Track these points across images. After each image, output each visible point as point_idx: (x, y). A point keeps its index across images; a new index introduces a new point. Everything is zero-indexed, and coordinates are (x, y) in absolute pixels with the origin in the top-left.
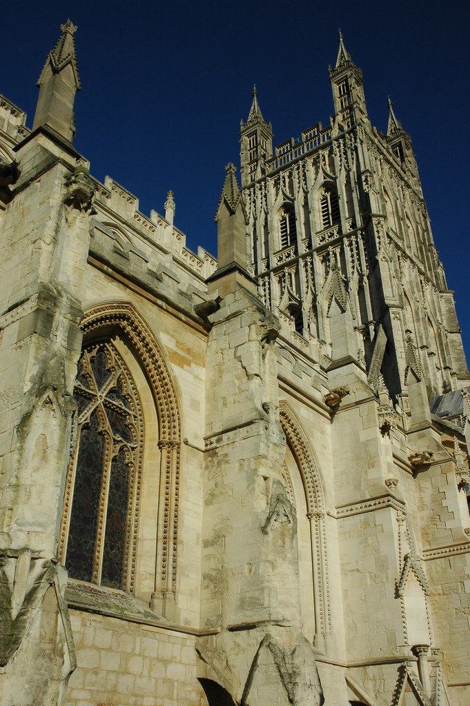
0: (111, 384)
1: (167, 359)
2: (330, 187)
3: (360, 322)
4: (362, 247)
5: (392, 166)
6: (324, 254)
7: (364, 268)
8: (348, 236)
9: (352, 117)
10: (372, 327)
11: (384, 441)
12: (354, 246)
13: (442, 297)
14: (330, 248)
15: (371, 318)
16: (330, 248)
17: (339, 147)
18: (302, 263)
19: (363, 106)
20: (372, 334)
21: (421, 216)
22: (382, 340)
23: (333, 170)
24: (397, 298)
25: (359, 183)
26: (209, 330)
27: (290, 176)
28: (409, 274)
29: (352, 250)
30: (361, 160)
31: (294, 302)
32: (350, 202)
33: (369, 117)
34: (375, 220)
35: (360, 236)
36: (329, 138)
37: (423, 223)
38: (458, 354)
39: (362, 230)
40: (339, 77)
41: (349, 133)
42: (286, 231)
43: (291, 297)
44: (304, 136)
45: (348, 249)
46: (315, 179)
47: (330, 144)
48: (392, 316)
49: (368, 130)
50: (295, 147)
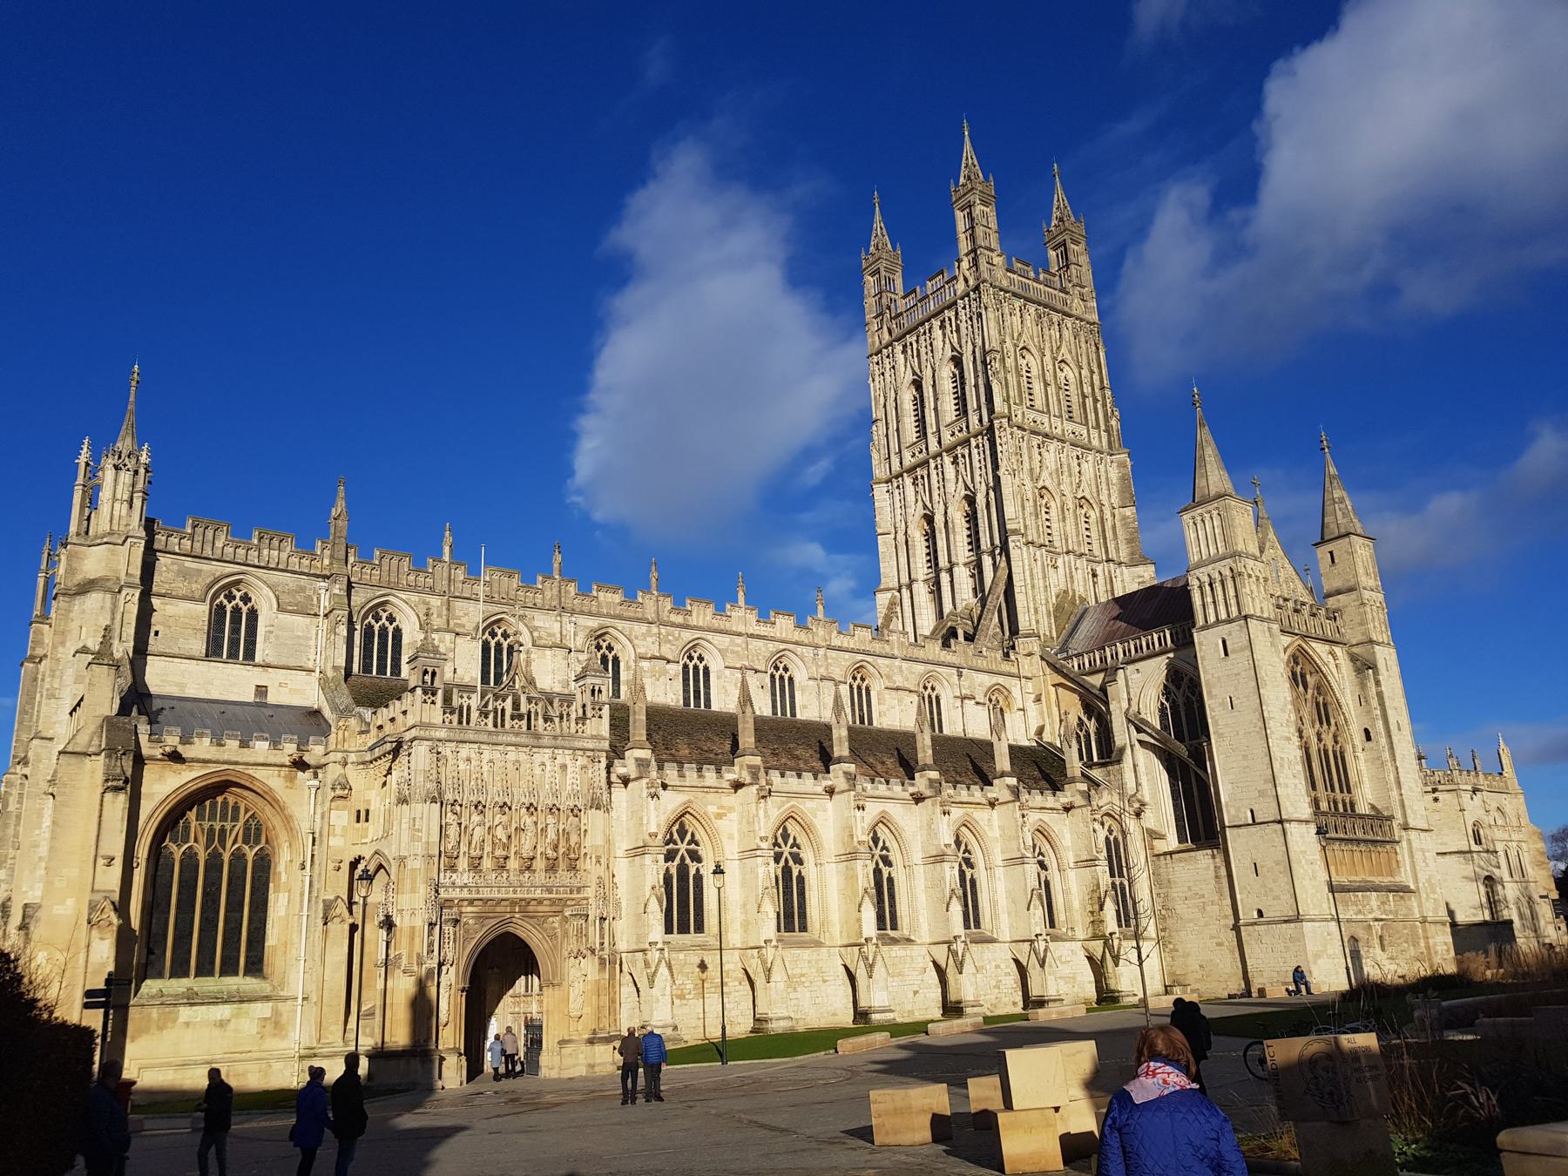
0: (688, 837)
1: (713, 819)
2: (957, 361)
4: (988, 452)
10: (997, 551)
11: (859, 813)
13: (1112, 462)
15: (997, 542)
18: (932, 465)
20: (998, 558)
22: (1003, 574)
25: (984, 363)
27: (917, 342)
30: (986, 334)
32: (976, 386)
34: (996, 422)
35: (985, 438)
40: (962, 202)
43: (925, 507)
44: (929, 284)
47: (955, 303)
48: (1011, 545)
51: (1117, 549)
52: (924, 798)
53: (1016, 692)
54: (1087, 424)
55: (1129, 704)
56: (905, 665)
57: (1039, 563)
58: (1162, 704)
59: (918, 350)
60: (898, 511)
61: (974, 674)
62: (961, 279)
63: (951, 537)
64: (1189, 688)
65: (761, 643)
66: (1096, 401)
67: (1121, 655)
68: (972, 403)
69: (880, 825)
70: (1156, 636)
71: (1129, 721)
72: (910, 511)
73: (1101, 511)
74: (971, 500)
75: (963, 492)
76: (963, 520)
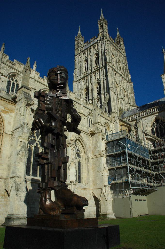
2: (97, 54)
3: (103, 92)
4: (104, 71)
5: (116, 47)
6: (95, 73)
7: (105, 77)
8: (101, 68)
9: (103, 34)
10: (106, 93)
12: (102, 71)
14: (96, 72)
15: (106, 91)
16: (96, 72)
17: (100, 43)
18: (89, 76)
19: (107, 31)
20: (106, 95)
21: (125, 61)
23: (98, 50)
24: (114, 85)
26: (16, 103)
28: (118, 78)
29: (102, 72)
30: (105, 47)
31: (87, 87)
32: (102, 58)
33: (109, 34)
34: (107, 64)
35: (104, 68)
36: (97, 40)
37: (125, 63)
38: (133, 100)
39: (104, 66)
40: (100, 23)
41: (102, 39)
42: (86, 67)
44: (91, 40)
45: (101, 72)
46: (93, 52)
47: (97, 42)
48: (110, 90)
49: (108, 38)
50: (89, 43)
51: (131, 102)
52: (95, 134)
53: (111, 125)
54: (124, 75)
55: (143, 128)
56: (83, 108)
57: (116, 98)
58: (152, 128)
59: (87, 53)
60: (79, 88)
61: (101, 117)
62: (99, 37)
63: (93, 91)
64: (161, 123)
65: (39, 84)
66: (126, 71)
67: (141, 116)
68: (101, 61)
69: (78, 141)
70: (152, 110)
71: (144, 132)
72: (83, 87)
73: (128, 93)
74: (99, 83)
75: (97, 81)
76: (96, 88)
